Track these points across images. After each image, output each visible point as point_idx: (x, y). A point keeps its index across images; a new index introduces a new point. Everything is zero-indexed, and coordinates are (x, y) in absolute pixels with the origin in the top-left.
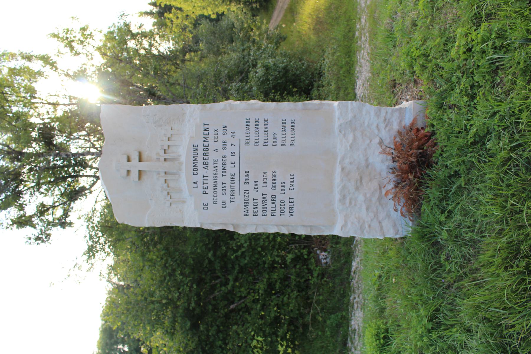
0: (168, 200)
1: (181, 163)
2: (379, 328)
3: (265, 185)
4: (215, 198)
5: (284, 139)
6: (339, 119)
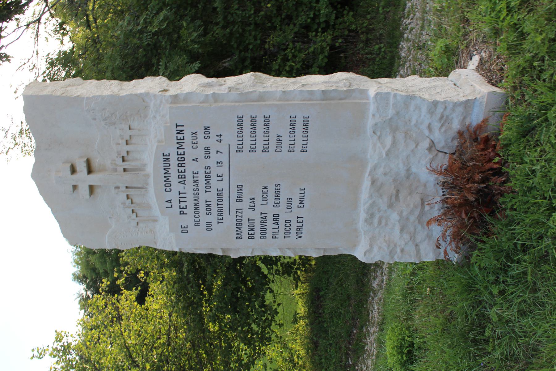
0: (134, 219)
1: (148, 176)
2: (403, 339)
3: (265, 202)
4: (197, 219)
5: (293, 143)
6: (373, 115)
